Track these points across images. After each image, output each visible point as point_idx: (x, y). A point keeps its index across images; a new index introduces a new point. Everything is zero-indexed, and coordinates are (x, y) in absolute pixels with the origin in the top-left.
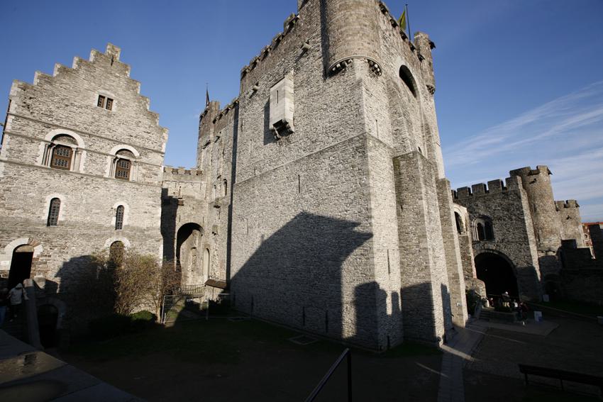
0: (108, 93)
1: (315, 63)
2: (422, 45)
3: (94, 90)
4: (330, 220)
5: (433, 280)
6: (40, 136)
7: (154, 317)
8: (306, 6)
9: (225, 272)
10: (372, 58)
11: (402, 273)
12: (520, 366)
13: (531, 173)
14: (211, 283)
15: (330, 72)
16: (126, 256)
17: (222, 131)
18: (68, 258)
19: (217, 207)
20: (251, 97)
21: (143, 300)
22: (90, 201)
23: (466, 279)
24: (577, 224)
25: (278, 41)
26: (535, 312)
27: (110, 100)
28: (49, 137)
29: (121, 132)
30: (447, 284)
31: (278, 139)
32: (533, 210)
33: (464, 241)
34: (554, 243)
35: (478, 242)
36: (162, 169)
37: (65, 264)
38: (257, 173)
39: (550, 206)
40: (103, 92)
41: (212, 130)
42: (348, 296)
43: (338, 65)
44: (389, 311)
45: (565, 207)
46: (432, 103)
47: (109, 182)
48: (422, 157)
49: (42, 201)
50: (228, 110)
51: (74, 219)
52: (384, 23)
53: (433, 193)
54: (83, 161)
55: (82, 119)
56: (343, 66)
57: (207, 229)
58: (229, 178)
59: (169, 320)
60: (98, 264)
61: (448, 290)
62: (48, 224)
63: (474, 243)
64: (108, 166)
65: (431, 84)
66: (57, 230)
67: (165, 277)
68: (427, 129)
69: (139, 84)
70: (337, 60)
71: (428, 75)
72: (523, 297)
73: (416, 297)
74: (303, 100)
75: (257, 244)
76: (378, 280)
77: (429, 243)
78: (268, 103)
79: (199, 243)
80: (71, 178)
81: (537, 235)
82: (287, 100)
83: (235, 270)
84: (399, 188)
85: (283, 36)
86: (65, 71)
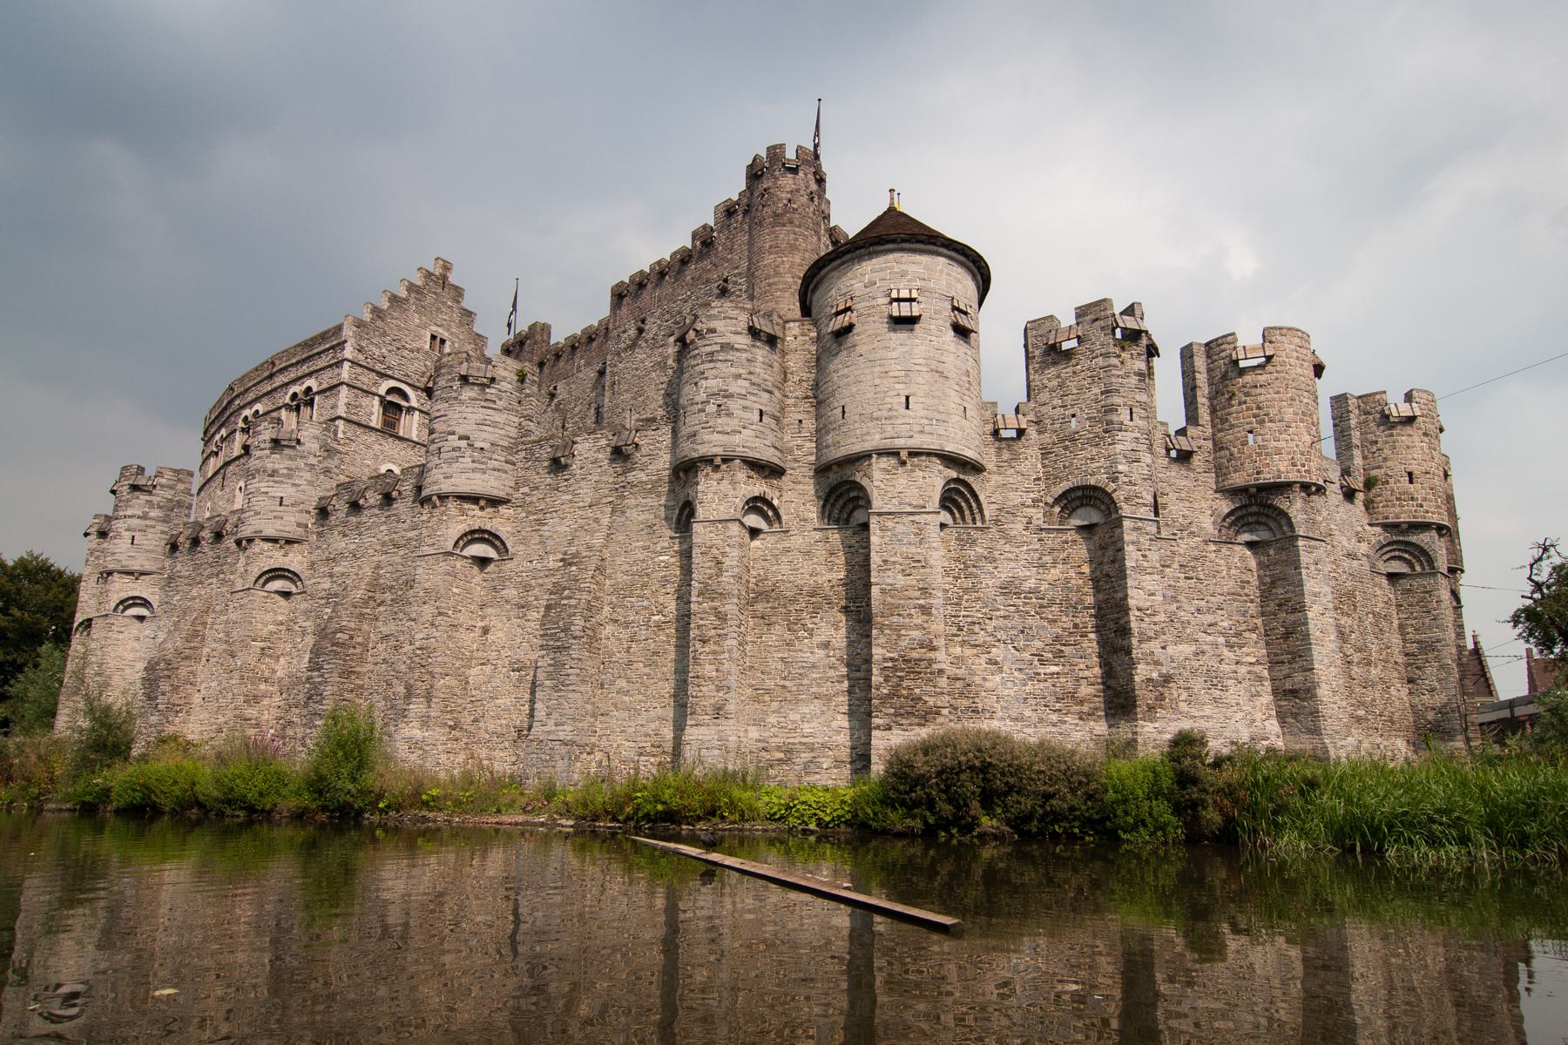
3: (425, 327)
27: (443, 341)
40: (434, 328)
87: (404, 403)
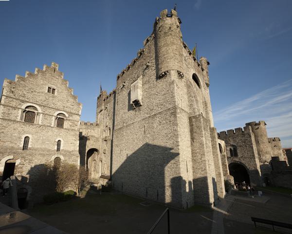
1: (152, 72)
2: (203, 64)
4: (159, 147)
5: (208, 175)
6: (19, 107)
7: (75, 193)
8: (148, 44)
9: (109, 171)
10: (179, 70)
11: (193, 172)
12: (252, 218)
13: (256, 124)
14: (103, 177)
15: (159, 77)
16: (62, 164)
17: (108, 105)
18: (33, 165)
19: (106, 141)
20: (121, 89)
21: (70, 185)
22: (44, 138)
23: (224, 175)
24: (280, 149)
25: (135, 62)
26: (259, 192)
27: (54, 90)
28: (24, 107)
29: (59, 105)
30: (215, 177)
31: (135, 109)
32: (257, 142)
33: (223, 157)
34: (268, 158)
35: (230, 157)
36: (79, 123)
37: (32, 168)
38: (125, 124)
39: (265, 140)
40: (50, 85)
41: (103, 104)
42: (168, 183)
43: (163, 73)
44: (187, 190)
45: (273, 141)
46: (208, 91)
47: (53, 129)
48: (203, 117)
49: (20, 138)
50: (111, 95)
51: (36, 147)
52: (185, 53)
53: (208, 134)
54: (41, 119)
55: (41, 98)
56: (165, 74)
57: (101, 151)
58: (111, 127)
59: (82, 195)
60: (48, 168)
61: (216, 180)
62: (23, 149)
63: (228, 158)
64: (53, 121)
65: (207, 82)
66: (28, 152)
67: (81, 174)
68: (205, 104)
69: (68, 83)
70: (163, 71)
71: (206, 78)
72: (252, 184)
73: (200, 184)
74: (147, 90)
75: (125, 158)
76: (182, 175)
77: (206, 158)
78: (130, 91)
80: (35, 127)
81: (259, 154)
82: (139, 90)
83: (114, 171)
84: (192, 131)
85: (137, 59)
86: (31, 75)
87: (35, 111)
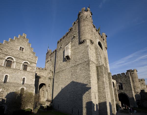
0: (23, 46)
1: (76, 40)
2: (104, 36)
3: (19, 46)
4: (80, 83)
5: (107, 101)
6: (4, 58)
7: (32, 110)
8: (75, 25)
9: (51, 97)
10: (91, 39)
11: (99, 99)
13: (132, 71)
14: (48, 101)
15: (81, 43)
16: (25, 92)
17: (52, 58)
18: (9, 92)
19: (50, 79)
20: (60, 49)
21: (29, 105)
22: (16, 76)
23: (116, 101)
24: (145, 85)
25: (67, 34)
26: (135, 111)
27: (23, 48)
28: (6, 58)
29: (25, 57)
30: (111, 102)
31: (67, 61)
32: (133, 81)
33: (115, 90)
34: (139, 91)
35: (119, 90)
36: (36, 68)
37: (8, 94)
38: (61, 70)
39: (137, 80)
40: (21, 46)
41: (49, 57)
42: (84, 105)
44: (95, 110)
45: (141, 81)
46: (106, 51)
47: (21, 71)
48: (104, 66)
49: (3, 76)
50: (54, 52)
51: (11, 81)
52: (94, 30)
53: (107, 77)
54: (15, 65)
55: (15, 53)
56: (84, 41)
57: (47, 85)
58: (53, 71)
59: (35, 111)
60: (17, 94)
61: (111, 104)
62: (4, 83)
63: (118, 90)
64: (21, 67)
65: (106, 47)
66: (6, 84)
67: (35, 99)
68: (105, 59)
69: (31, 44)
70: (83, 39)
71: (105, 44)
72: (131, 106)
73: (103, 106)
74: (73, 50)
75: (60, 90)
76: (92, 101)
77: (106, 91)
78: (64, 51)
79: (45, 89)
81: (134, 88)
83: (54, 97)
84: (98, 75)
85: (68, 33)
86: (12, 40)
87: (12, 61)
